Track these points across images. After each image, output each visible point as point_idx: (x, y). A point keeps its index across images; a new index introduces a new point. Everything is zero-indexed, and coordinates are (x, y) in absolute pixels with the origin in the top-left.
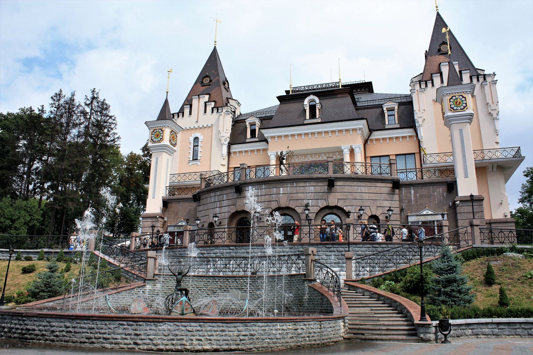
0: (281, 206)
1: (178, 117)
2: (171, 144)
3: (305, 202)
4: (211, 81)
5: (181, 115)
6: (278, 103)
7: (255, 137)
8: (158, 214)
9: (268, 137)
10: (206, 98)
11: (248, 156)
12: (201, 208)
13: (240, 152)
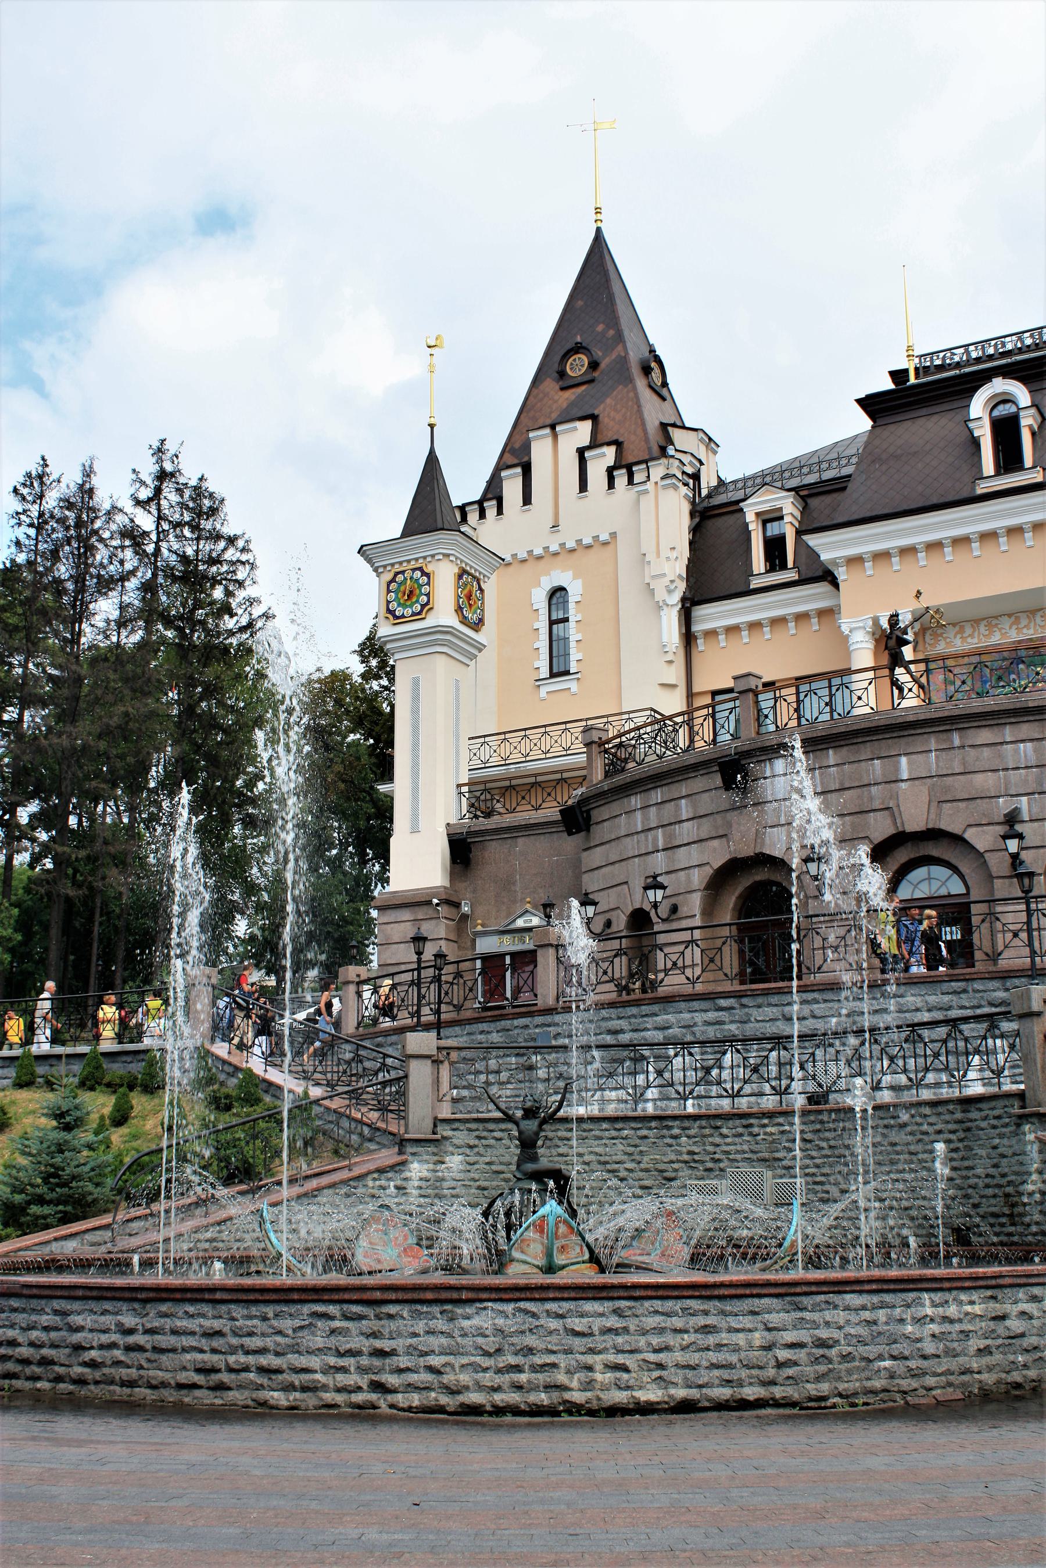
0: (911, 827)
1: (482, 515)
2: (464, 621)
3: (1004, 805)
4: (594, 365)
5: (491, 507)
6: (864, 423)
7: (784, 566)
8: (433, 892)
9: (834, 561)
10: (583, 432)
11: (759, 641)
12: (597, 857)
13: (732, 630)
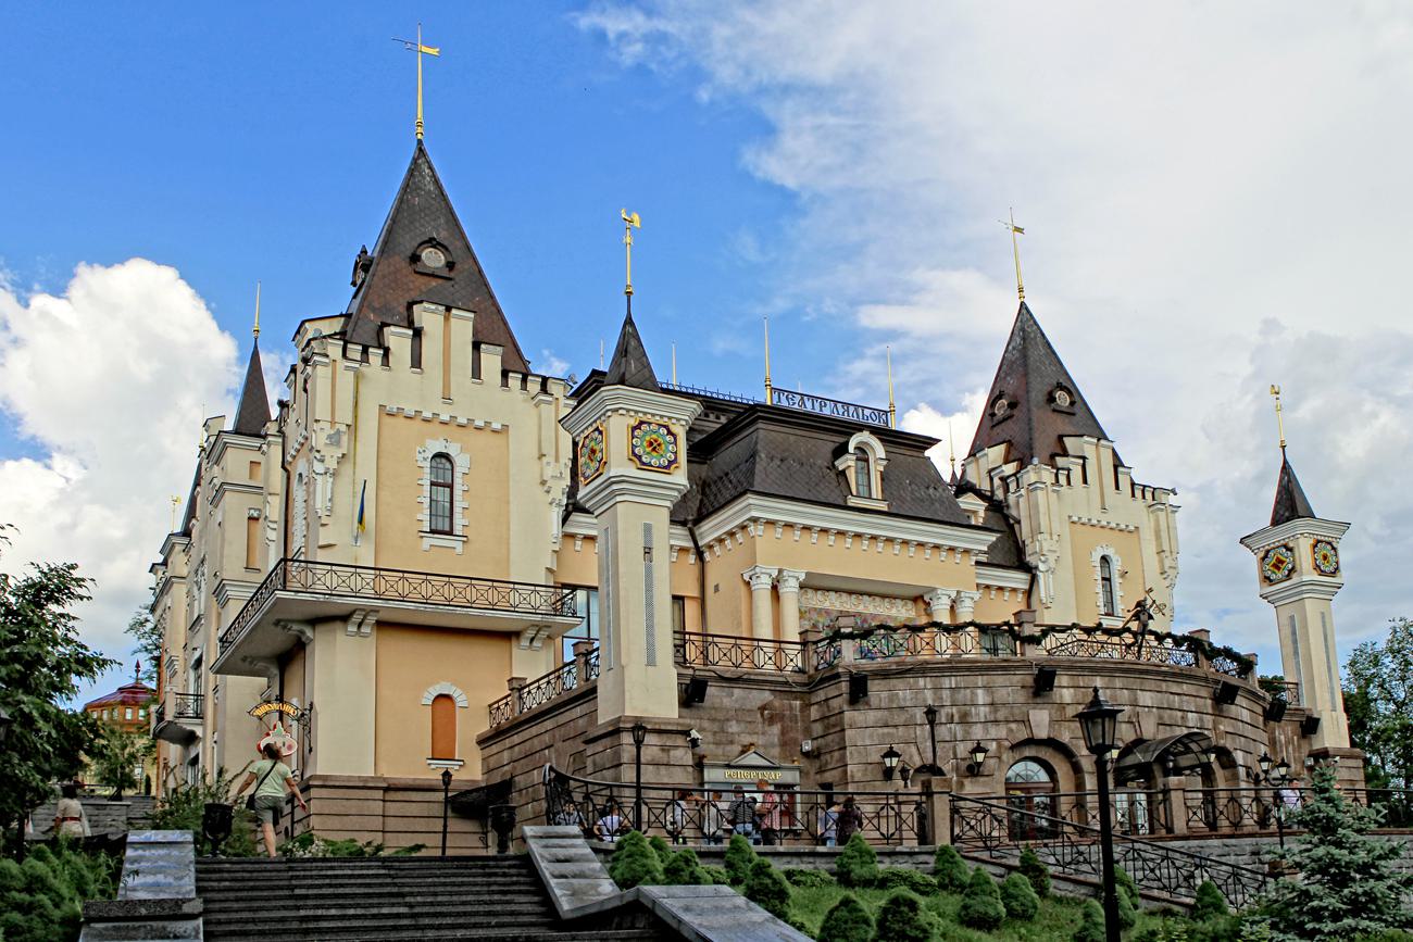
9: (755, 520)
